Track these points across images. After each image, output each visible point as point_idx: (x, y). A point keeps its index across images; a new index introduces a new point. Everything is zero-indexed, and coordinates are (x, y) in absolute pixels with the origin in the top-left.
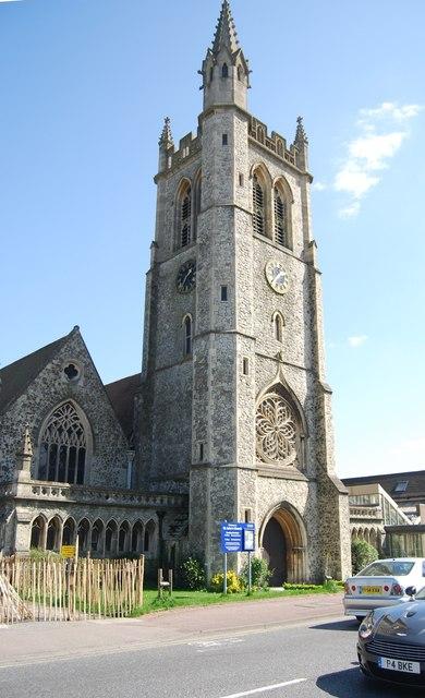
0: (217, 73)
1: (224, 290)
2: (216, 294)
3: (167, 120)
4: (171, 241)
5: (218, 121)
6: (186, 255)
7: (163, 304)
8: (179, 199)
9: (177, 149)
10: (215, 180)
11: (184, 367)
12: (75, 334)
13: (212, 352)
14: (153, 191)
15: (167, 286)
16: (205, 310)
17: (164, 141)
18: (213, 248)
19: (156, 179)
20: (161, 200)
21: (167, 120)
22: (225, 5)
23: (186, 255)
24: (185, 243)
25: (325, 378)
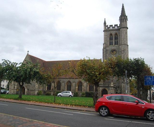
0: (125, 20)
3: (105, 19)
4: (109, 44)
6: (113, 47)
7: (107, 55)
8: (109, 36)
9: (109, 26)
10: (125, 40)
14: (103, 34)
15: (109, 52)
17: (105, 23)
18: (126, 52)
19: (104, 31)
20: (105, 35)
21: (105, 19)
22: (123, 5)
23: (113, 47)
24: (110, 44)
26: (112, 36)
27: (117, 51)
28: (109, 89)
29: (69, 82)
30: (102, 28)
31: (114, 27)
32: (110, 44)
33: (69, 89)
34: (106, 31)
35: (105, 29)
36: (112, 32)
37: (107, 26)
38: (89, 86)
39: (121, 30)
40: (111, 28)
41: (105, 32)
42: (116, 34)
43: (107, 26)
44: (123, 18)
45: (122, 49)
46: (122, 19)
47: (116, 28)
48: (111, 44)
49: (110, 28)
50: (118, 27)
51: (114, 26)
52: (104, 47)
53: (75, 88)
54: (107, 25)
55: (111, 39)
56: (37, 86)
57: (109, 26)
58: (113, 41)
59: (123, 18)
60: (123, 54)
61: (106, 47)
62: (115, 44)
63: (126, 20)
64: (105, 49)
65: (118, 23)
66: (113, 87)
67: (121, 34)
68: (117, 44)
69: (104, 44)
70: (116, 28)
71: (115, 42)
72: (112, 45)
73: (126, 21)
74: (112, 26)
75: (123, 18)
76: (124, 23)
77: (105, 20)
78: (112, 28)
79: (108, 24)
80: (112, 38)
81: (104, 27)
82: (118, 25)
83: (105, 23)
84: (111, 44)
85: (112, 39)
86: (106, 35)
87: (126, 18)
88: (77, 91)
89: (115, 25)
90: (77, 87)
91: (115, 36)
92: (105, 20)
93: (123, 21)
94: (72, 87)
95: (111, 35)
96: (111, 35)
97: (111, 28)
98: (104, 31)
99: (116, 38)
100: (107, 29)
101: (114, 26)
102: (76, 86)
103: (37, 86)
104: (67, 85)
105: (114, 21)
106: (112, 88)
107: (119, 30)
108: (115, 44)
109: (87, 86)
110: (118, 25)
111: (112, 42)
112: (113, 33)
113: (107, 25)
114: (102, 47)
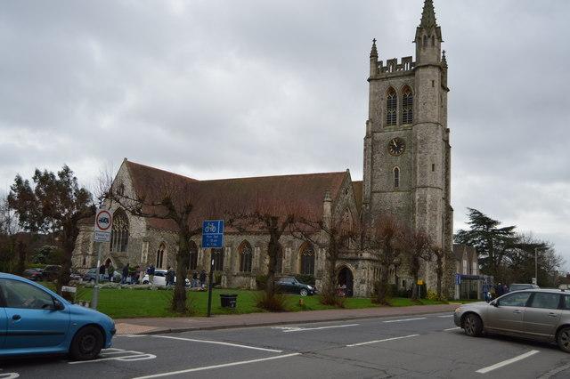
1: (433, 165)
2: (430, 168)
3: (374, 41)
4: (383, 121)
5: (430, 73)
7: (378, 157)
8: (385, 96)
9: (385, 65)
10: (428, 107)
11: (395, 194)
12: (347, 175)
13: (429, 196)
15: (381, 148)
16: (424, 175)
17: (374, 54)
18: (429, 145)
19: (369, 80)
20: (372, 94)
21: (374, 41)
24: (388, 123)
25: (452, 204)
26: (395, 97)
28: (357, 267)
29: (246, 243)
30: (366, 70)
31: (402, 66)
32: (388, 123)
33: (246, 266)
34: (376, 80)
35: (373, 74)
36: (392, 82)
37: (381, 62)
38: (302, 256)
39: (417, 73)
41: (372, 82)
42: (407, 88)
43: (381, 62)
44: (428, 32)
45: (419, 138)
46: (420, 39)
48: (390, 120)
49: (387, 68)
50: (412, 64)
51: (399, 62)
52: (367, 133)
53: (261, 263)
54: (379, 60)
55: (391, 104)
56: (144, 258)
57: (385, 65)
58: (398, 112)
59: (425, 33)
60: (420, 152)
61: (373, 132)
63: (436, 40)
64: (370, 139)
65: (411, 51)
66: (368, 260)
67: (418, 90)
68: (410, 122)
69: (367, 123)
70: (407, 67)
72: (395, 123)
73: (433, 44)
74: (392, 62)
75: (428, 32)
76: (429, 49)
77: (374, 45)
79: (383, 57)
80: (395, 101)
81: (371, 67)
82: (414, 60)
83: (374, 54)
84: (390, 120)
86: (376, 94)
87: (434, 33)
88: (266, 270)
89: (406, 60)
90: (267, 261)
91: (406, 97)
92: (374, 45)
93: (425, 45)
94: (316, 261)
95: (391, 90)
96: (391, 90)
98: (369, 80)
99: (408, 102)
100: (380, 72)
101: (399, 62)
102: (262, 258)
103: (144, 258)
104: (242, 255)
105: (400, 45)
106: (367, 264)
107: (412, 73)
108: (404, 121)
109: (293, 258)
110: (414, 60)
112: (398, 84)
113: (379, 60)
114: (362, 131)
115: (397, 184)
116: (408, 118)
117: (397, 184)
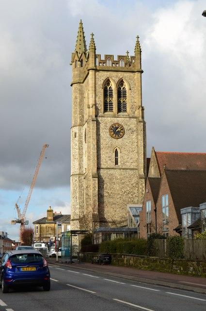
24: (105, 110)
27: (125, 127)
31: (117, 63)
40: (109, 64)
42: (121, 83)
47: (122, 64)
55: (107, 93)
62: (119, 110)
71: (119, 103)
72: (111, 110)
74: (109, 57)
78: (113, 63)
79: (102, 52)
84: (107, 107)
85: (111, 96)
89: (120, 57)
95: (107, 82)
96: (107, 82)
97: (109, 64)
99: (121, 94)
101: (116, 59)
111: (111, 104)
112: (114, 78)
115: (116, 163)
116: (121, 108)
117: (116, 163)
